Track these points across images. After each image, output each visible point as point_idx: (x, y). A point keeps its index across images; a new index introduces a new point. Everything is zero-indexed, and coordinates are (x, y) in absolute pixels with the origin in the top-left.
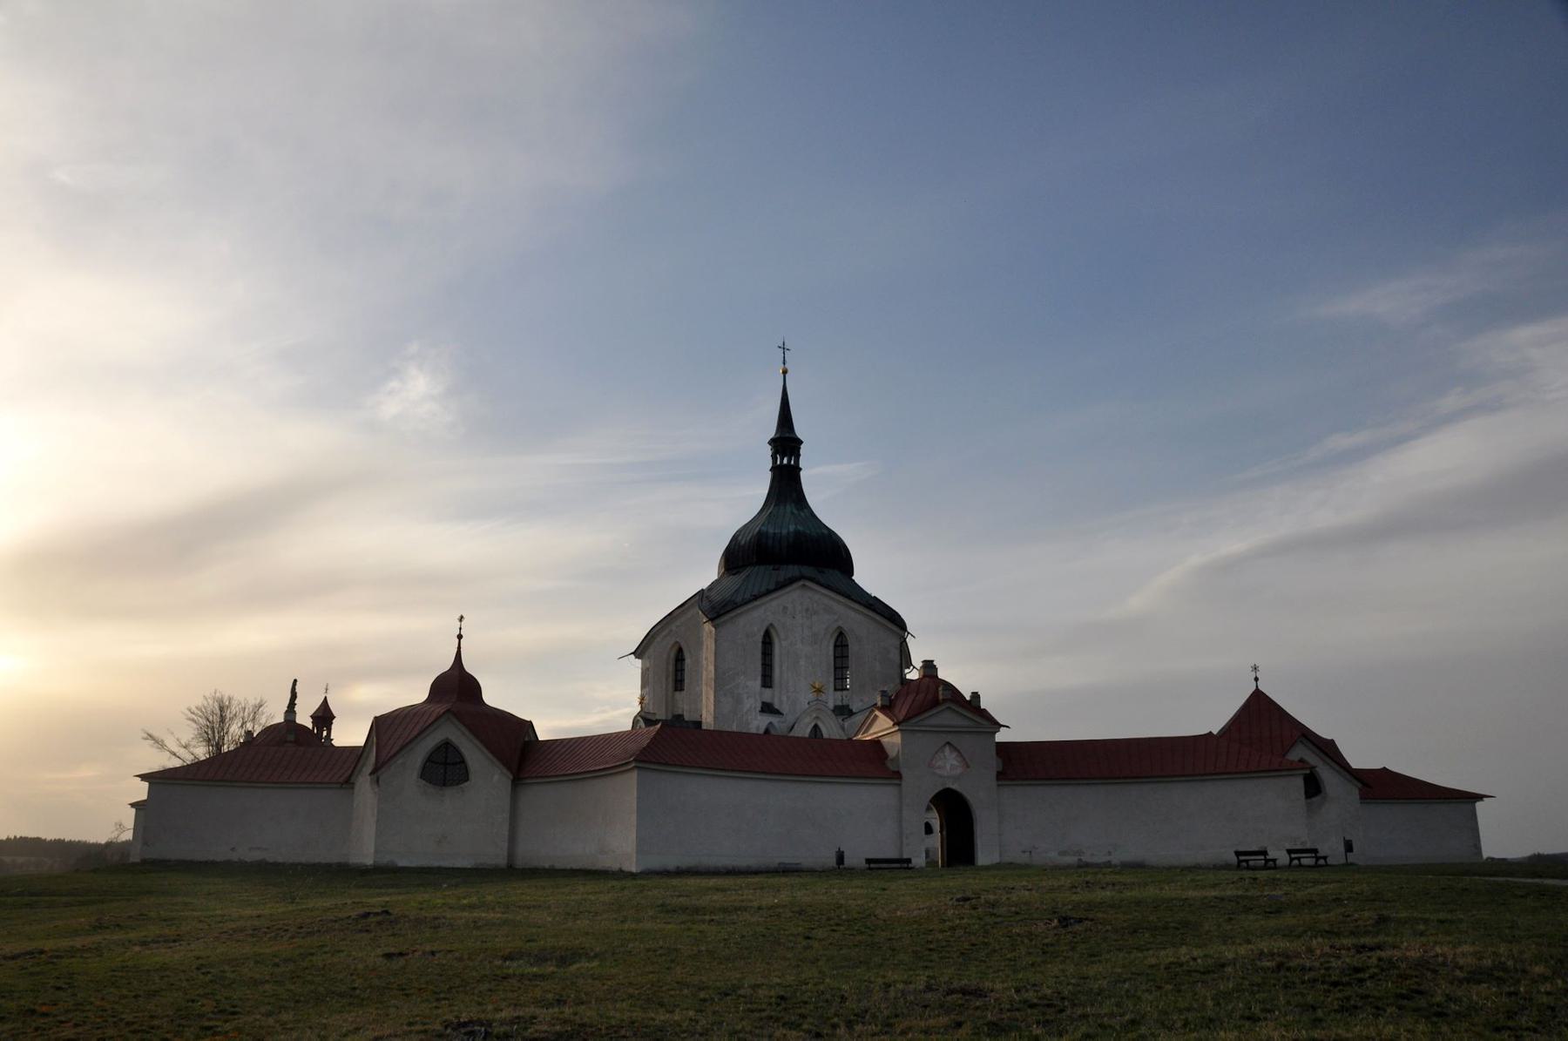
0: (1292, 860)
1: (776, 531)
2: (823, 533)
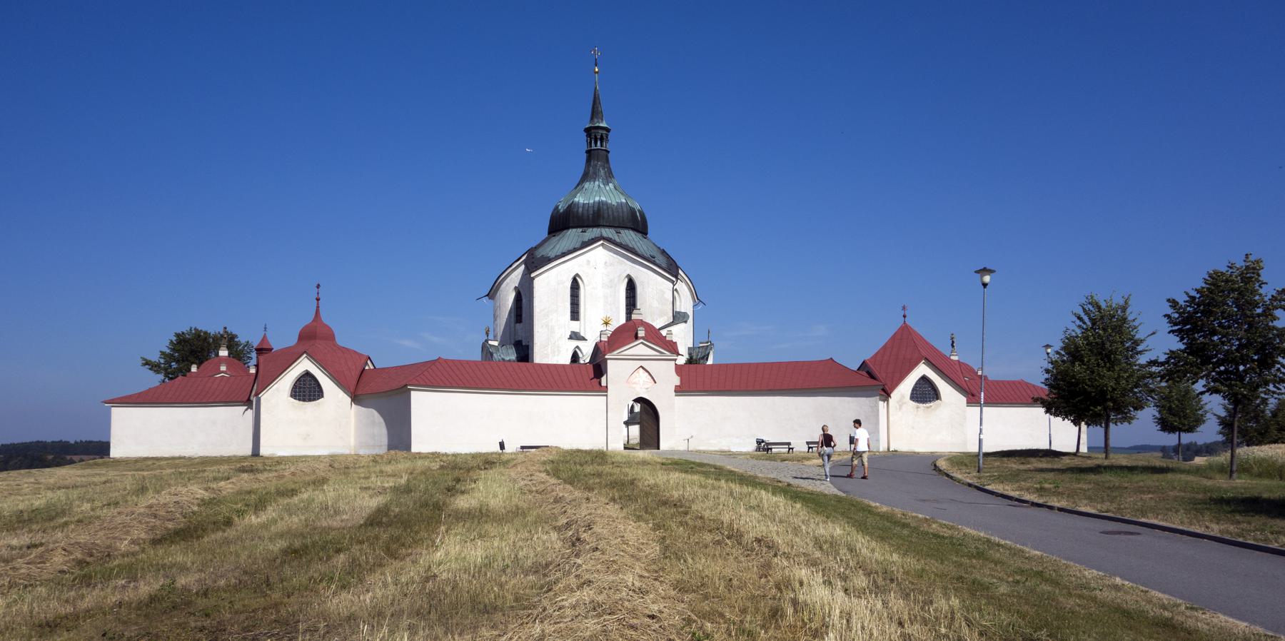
0: (809, 448)
1: (585, 202)
2: (621, 203)
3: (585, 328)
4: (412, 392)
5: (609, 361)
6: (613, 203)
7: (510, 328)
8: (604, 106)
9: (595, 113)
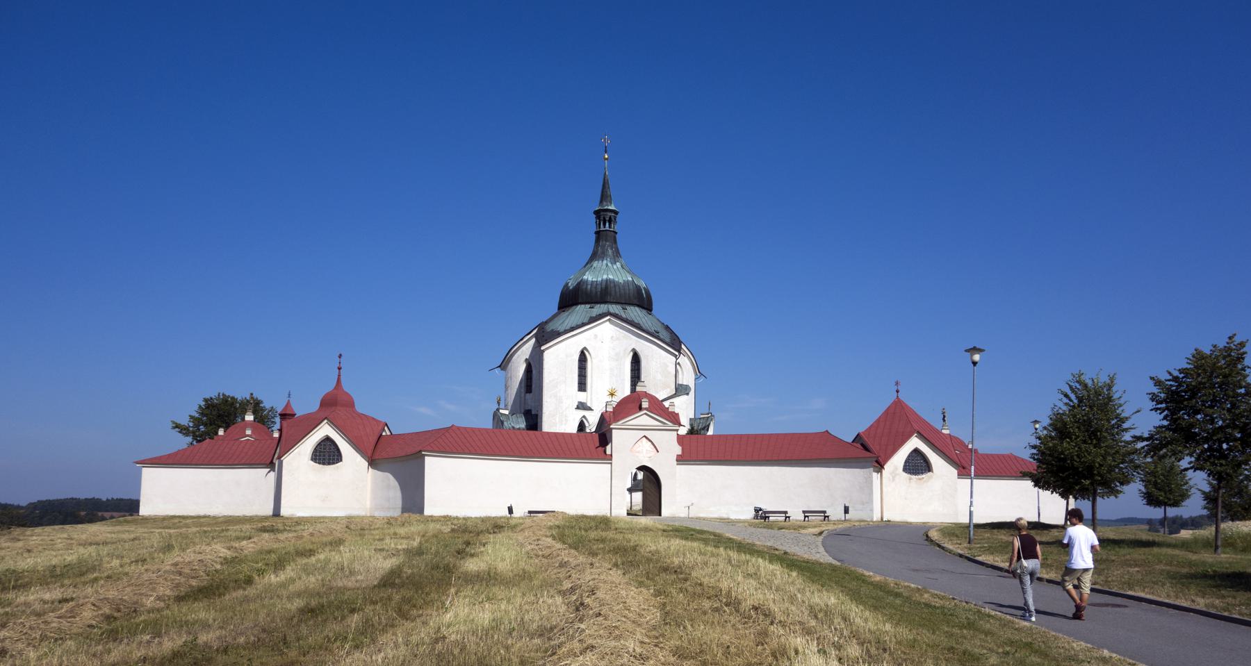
0: (805, 517)
2: (628, 281)
3: (591, 399)
4: (426, 457)
5: (613, 431)
6: (620, 281)
7: (521, 397)
8: (613, 191)
9: (605, 197)
